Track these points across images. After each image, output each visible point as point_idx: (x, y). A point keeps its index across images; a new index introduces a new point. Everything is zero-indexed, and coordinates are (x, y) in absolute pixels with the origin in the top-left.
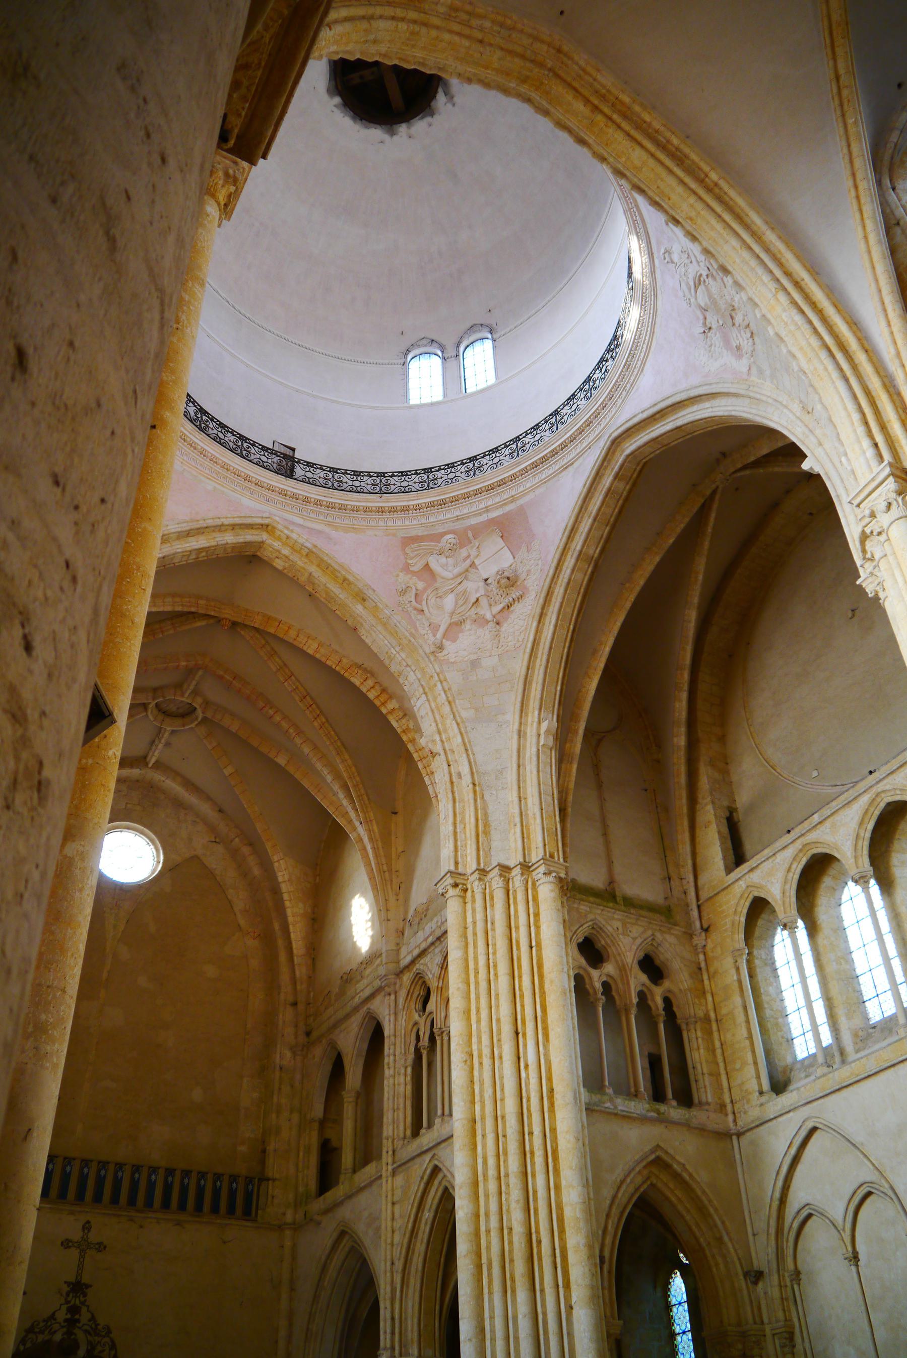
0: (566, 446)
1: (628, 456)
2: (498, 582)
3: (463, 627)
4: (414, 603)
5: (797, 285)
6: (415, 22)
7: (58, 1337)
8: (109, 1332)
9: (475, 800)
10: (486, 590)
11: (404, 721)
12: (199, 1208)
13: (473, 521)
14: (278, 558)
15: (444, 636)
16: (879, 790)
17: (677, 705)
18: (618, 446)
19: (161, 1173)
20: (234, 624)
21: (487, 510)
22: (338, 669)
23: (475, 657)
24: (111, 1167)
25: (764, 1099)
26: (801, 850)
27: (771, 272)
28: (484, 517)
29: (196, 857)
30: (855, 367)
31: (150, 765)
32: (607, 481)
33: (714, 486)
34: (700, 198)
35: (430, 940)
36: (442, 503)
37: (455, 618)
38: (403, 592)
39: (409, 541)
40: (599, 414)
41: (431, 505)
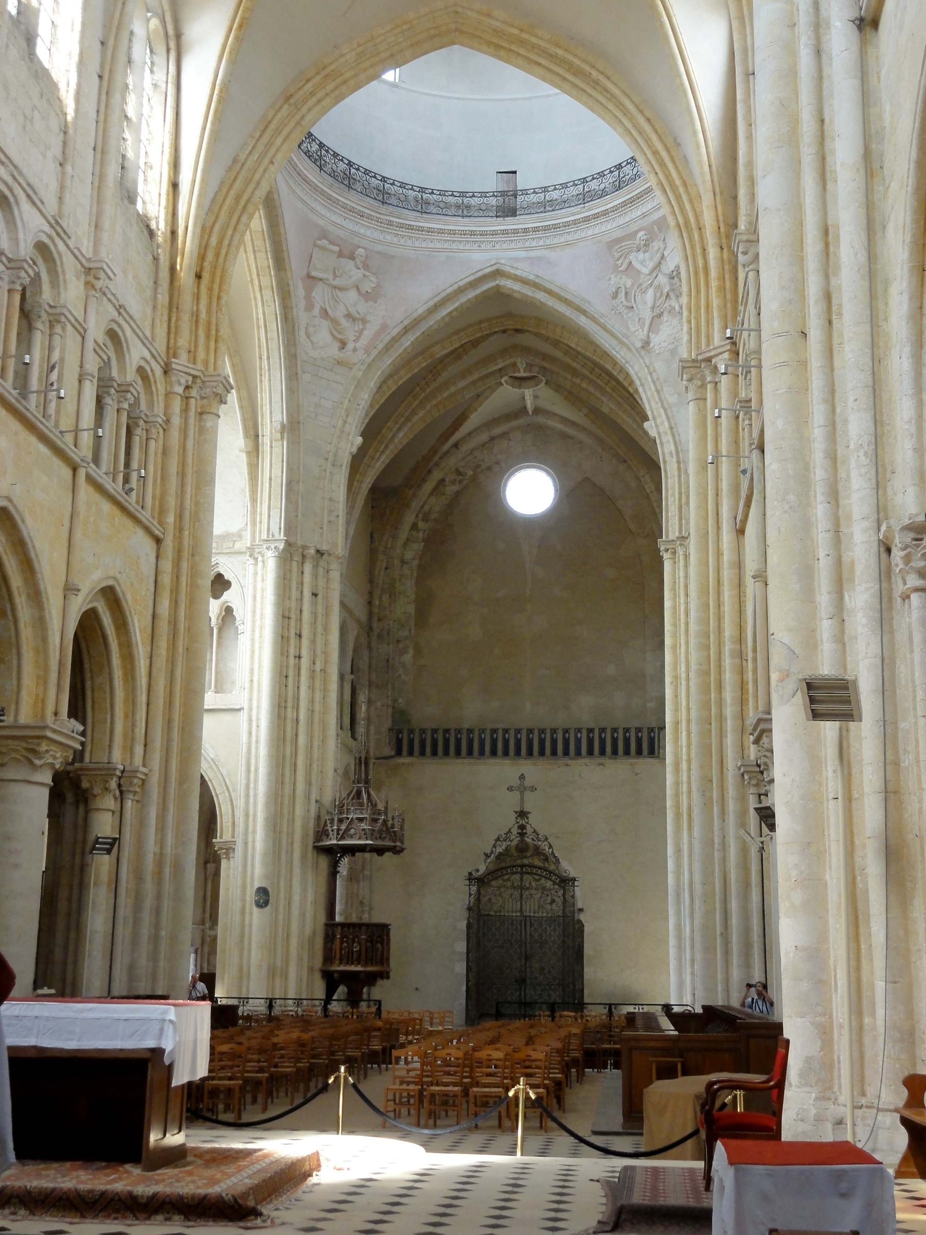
4: (625, 303)
5: (662, 164)
6: (336, 88)
7: (515, 843)
8: (546, 839)
9: (680, 476)
10: (672, 285)
12: (615, 752)
15: (649, 331)
19: (584, 732)
23: (672, 347)
24: (548, 731)
27: (645, 154)
29: (587, 478)
30: (693, 247)
31: (530, 413)
34: (590, 96)
36: (632, 201)
37: (657, 311)
38: (615, 295)
41: (624, 204)
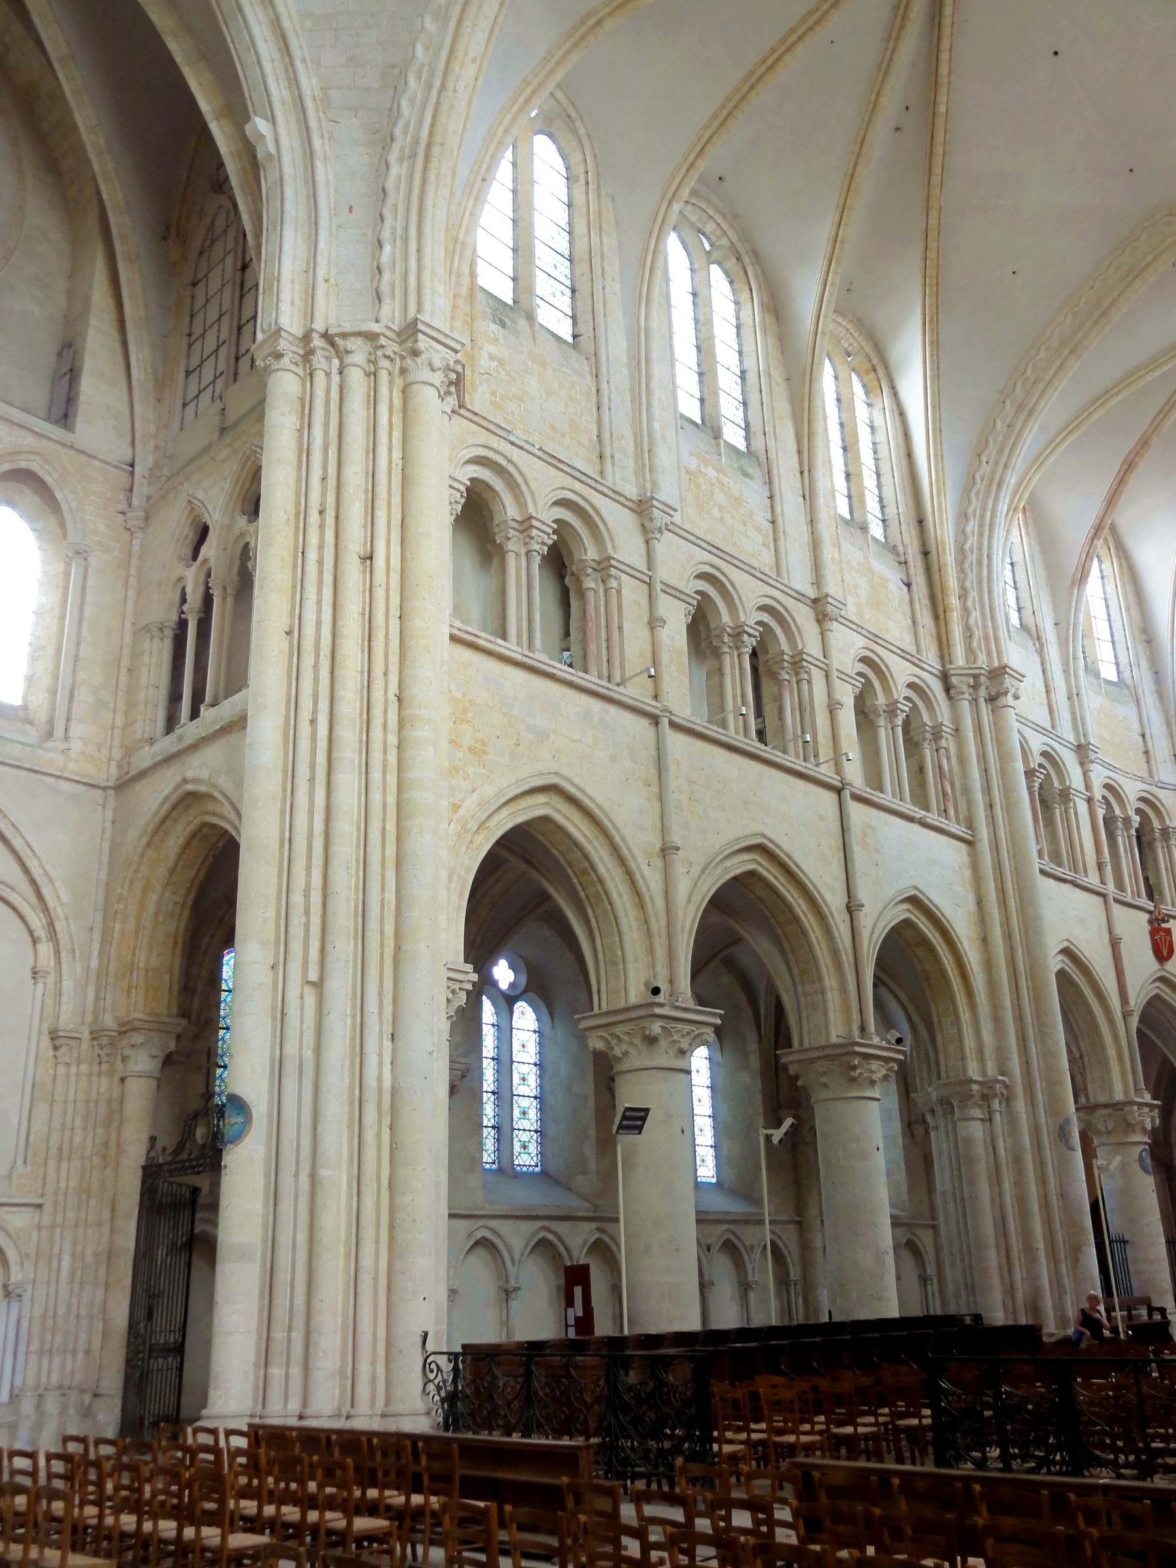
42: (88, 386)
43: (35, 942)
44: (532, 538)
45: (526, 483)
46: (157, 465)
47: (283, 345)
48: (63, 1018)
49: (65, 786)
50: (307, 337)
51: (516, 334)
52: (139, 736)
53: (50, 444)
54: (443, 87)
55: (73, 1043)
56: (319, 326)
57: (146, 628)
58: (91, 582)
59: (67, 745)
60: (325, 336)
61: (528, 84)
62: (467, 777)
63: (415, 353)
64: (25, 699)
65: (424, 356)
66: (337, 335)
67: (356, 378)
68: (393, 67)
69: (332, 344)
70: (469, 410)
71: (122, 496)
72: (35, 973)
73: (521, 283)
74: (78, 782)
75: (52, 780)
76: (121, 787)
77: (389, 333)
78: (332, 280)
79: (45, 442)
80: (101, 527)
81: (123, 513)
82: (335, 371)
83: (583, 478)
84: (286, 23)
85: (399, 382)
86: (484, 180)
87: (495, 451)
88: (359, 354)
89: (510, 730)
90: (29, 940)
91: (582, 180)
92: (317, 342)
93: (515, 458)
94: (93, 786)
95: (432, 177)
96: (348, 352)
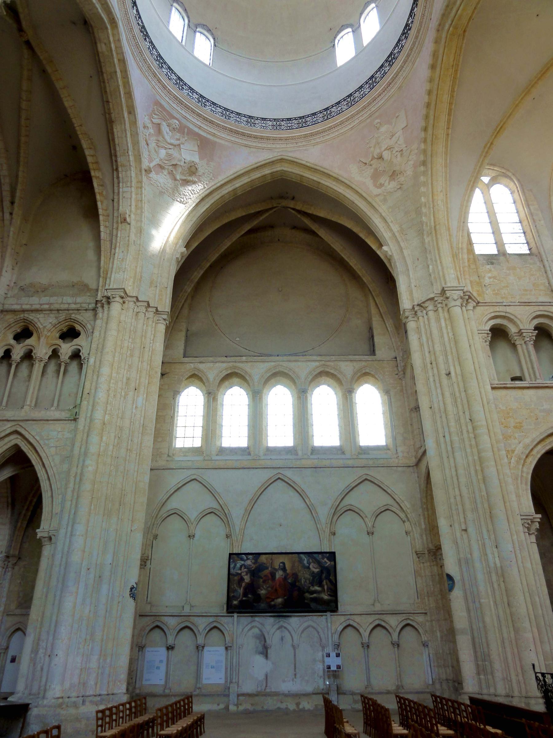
0: (250, 137)
1: (283, 170)
2: (191, 167)
3: (163, 171)
11: (101, 188)
13: (191, 126)
14: (105, 44)
16: (280, 364)
17: (195, 273)
18: (280, 162)
20: (28, 43)
21: (200, 128)
22: (77, 128)
25: (168, 459)
26: (231, 367)
28: (196, 130)
32: (267, 171)
33: (278, 205)
35: (46, 307)
39: (157, 103)
40: (276, 140)
42: (377, 339)
43: (404, 522)
44: (525, 337)
45: (516, 317)
46: (403, 356)
47: (407, 314)
48: (417, 547)
49: (400, 469)
50: (413, 308)
51: (499, 264)
52: (418, 446)
53: (370, 362)
54: (434, 206)
55: (423, 555)
56: (416, 303)
57: (412, 410)
58: (393, 400)
59: (398, 455)
60: (418, 305)
61: (471, 181)
62: (515, 438)
63: (447, 298)
64: (386, 442)
65: (451, 297)
66: (421, 303)
67: (431, 314)
68: (418, 208)
69: (422, 306)
70: (482, 303)
71: (396, 369)
72: (406, 533)
73: (498, 243)
74: (403, 466)
75: (395, 468)
76: (417, 464)
77: (437, 295)
78: (417, 285)
79: (368, 362)
80: (392, 382)
81: (397, 374)
82: (425, 315)
83: (543, 304)
84: (383, 214)
85: (446, 309)
86: (464, 222)
87: (499, 312)
88: (430, 306)
89: (532, 414)
90: (402, 522)
91: (516, 191)
92: (416, 308)
93: (508, 311)
94: (409, 466)
95: (439, 236)
96: (426, 307)
